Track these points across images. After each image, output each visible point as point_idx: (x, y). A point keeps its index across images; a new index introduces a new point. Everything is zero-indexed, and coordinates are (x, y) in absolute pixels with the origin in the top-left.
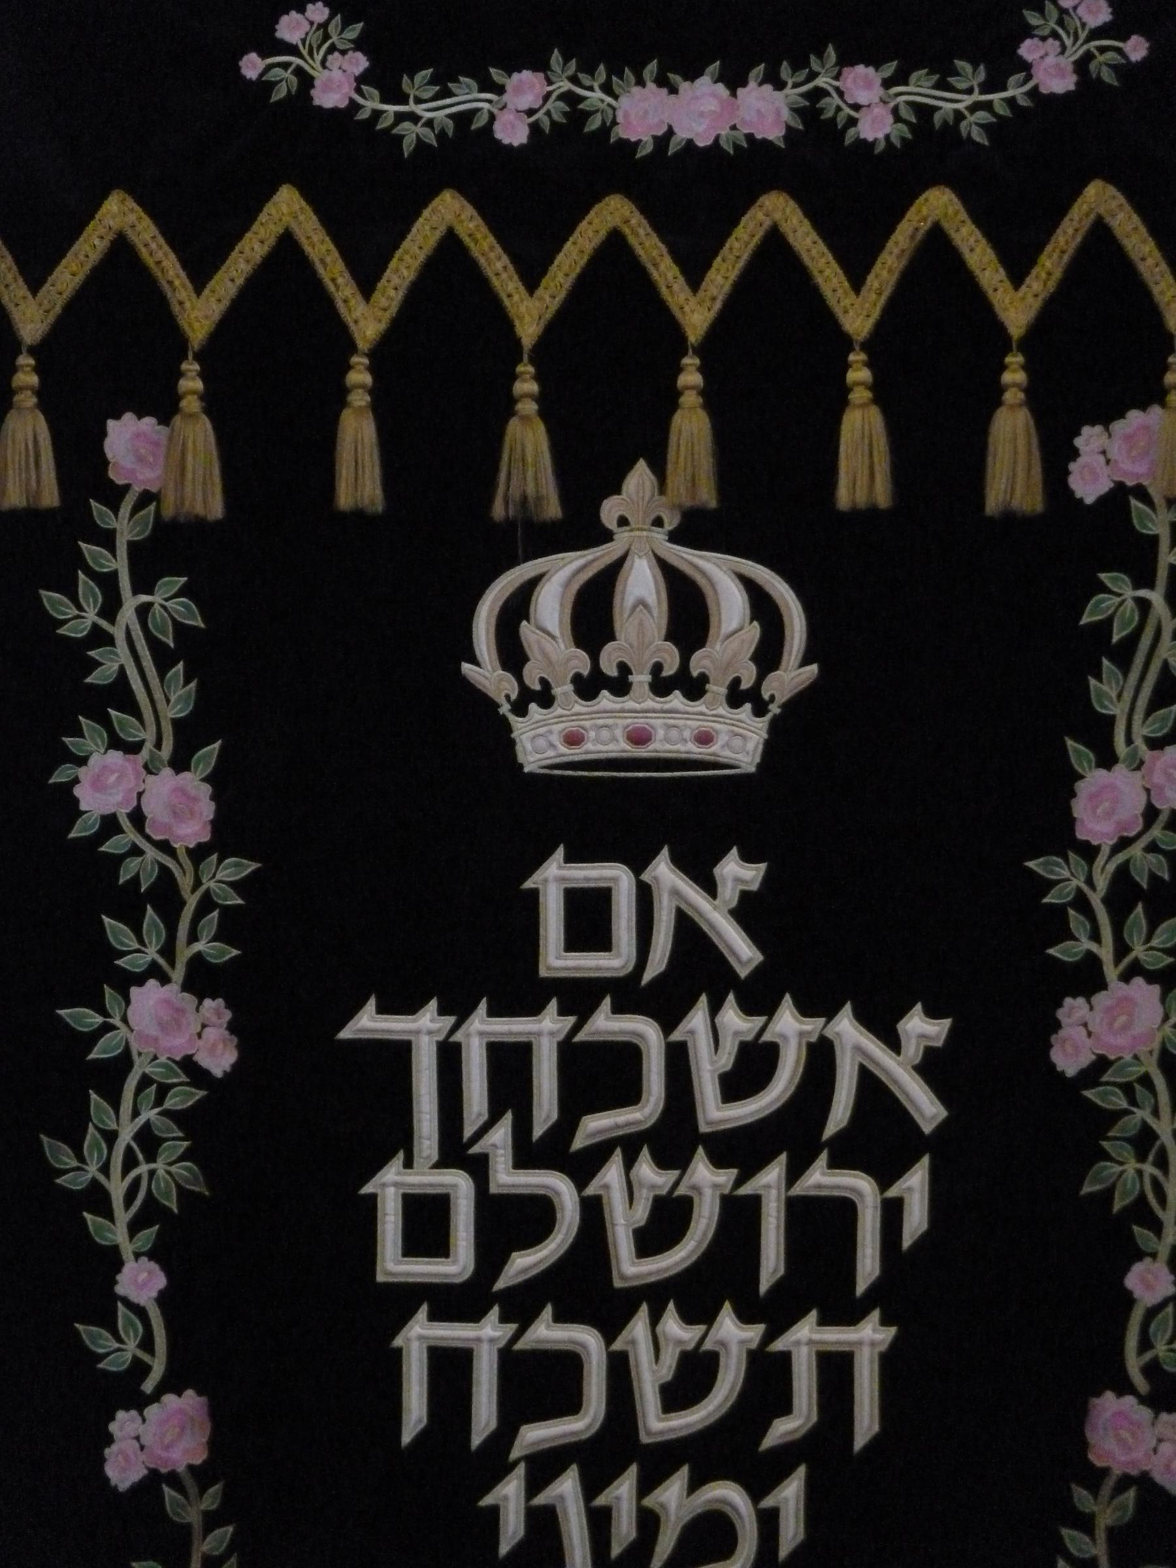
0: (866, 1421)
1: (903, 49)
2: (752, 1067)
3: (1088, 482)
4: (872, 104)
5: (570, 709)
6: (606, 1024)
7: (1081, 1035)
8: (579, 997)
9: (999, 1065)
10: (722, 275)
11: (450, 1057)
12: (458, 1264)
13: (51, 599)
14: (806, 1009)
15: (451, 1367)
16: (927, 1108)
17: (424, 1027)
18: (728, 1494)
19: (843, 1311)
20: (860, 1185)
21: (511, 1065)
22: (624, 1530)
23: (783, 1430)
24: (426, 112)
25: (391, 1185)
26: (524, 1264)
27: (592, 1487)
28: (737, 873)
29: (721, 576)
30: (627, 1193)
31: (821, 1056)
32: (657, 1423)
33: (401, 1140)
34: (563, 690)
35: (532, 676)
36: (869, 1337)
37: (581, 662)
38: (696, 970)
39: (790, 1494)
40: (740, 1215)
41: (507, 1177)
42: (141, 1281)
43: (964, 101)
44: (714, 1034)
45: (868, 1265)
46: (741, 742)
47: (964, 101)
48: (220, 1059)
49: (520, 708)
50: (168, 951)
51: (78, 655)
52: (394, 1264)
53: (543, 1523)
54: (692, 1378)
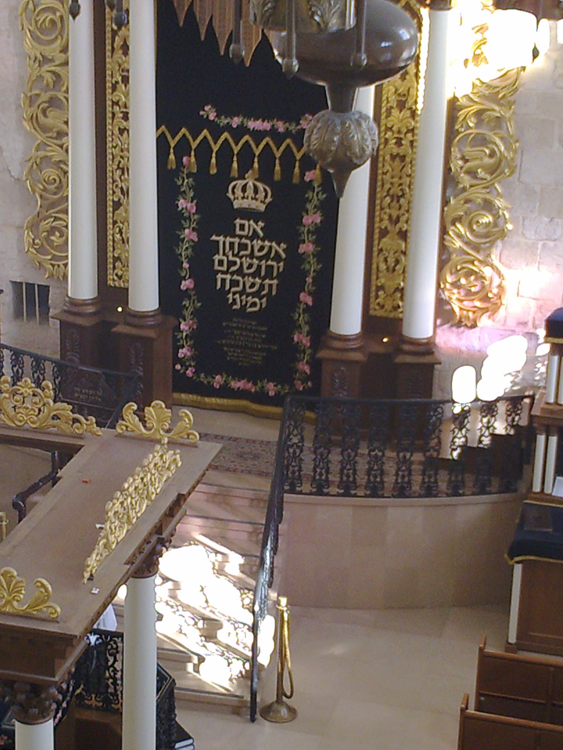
0: (274, 293)
1: (286, 119)
2: (262, 249)
3: (307, 178)
4: (281, 127)
5: (240, 201)
6: (244, 241)
7: (302, 248)
8: (241, 237)
9: (292, 250)
10: (261, 147)
11: (224, 243)
12: (225, 268)
13: (176, 179)
14: (269, 241)
15: (223, 280)
16: (284, 256)
17: (221, 239)
18: (256, 300)
19: (272, 279)
20: (274, 263)
21: (232, 244)
22: (244, 303)
23: (264, 293)
24: (224, 121)
25: (217, 258)
26: (233, 269)
27: (240, 296)
28: (261, 224)
29: (260, 186)
30: (246, 262)
31: (271, 247)
32: (249, 291)
33: (218, 253)
34: (240, 198)
35: (236, 196)
36: (275, 282)
37: (242, 195)
38: (255, 235)
39: (264, 300)
40: (259, 267)
41: (231, 258)
42: (186, 265)
43: (293, 128)
44: (257, 244)
45: (275, 274)
46: (262, 208)
47: (293, 128)
48: (196, 239)
49: (234, 199)
50: (190, 225)
51: (179, 187)
52: (217, 267)
53: (234, 300)
54: (253, 285)
